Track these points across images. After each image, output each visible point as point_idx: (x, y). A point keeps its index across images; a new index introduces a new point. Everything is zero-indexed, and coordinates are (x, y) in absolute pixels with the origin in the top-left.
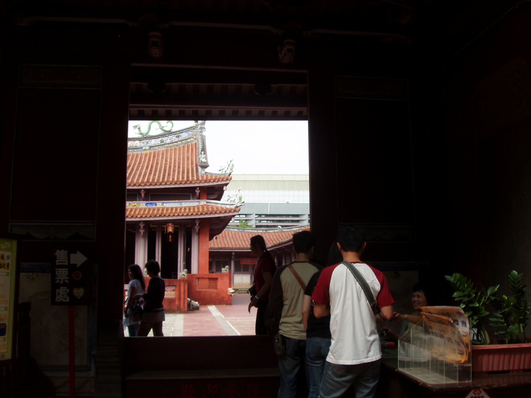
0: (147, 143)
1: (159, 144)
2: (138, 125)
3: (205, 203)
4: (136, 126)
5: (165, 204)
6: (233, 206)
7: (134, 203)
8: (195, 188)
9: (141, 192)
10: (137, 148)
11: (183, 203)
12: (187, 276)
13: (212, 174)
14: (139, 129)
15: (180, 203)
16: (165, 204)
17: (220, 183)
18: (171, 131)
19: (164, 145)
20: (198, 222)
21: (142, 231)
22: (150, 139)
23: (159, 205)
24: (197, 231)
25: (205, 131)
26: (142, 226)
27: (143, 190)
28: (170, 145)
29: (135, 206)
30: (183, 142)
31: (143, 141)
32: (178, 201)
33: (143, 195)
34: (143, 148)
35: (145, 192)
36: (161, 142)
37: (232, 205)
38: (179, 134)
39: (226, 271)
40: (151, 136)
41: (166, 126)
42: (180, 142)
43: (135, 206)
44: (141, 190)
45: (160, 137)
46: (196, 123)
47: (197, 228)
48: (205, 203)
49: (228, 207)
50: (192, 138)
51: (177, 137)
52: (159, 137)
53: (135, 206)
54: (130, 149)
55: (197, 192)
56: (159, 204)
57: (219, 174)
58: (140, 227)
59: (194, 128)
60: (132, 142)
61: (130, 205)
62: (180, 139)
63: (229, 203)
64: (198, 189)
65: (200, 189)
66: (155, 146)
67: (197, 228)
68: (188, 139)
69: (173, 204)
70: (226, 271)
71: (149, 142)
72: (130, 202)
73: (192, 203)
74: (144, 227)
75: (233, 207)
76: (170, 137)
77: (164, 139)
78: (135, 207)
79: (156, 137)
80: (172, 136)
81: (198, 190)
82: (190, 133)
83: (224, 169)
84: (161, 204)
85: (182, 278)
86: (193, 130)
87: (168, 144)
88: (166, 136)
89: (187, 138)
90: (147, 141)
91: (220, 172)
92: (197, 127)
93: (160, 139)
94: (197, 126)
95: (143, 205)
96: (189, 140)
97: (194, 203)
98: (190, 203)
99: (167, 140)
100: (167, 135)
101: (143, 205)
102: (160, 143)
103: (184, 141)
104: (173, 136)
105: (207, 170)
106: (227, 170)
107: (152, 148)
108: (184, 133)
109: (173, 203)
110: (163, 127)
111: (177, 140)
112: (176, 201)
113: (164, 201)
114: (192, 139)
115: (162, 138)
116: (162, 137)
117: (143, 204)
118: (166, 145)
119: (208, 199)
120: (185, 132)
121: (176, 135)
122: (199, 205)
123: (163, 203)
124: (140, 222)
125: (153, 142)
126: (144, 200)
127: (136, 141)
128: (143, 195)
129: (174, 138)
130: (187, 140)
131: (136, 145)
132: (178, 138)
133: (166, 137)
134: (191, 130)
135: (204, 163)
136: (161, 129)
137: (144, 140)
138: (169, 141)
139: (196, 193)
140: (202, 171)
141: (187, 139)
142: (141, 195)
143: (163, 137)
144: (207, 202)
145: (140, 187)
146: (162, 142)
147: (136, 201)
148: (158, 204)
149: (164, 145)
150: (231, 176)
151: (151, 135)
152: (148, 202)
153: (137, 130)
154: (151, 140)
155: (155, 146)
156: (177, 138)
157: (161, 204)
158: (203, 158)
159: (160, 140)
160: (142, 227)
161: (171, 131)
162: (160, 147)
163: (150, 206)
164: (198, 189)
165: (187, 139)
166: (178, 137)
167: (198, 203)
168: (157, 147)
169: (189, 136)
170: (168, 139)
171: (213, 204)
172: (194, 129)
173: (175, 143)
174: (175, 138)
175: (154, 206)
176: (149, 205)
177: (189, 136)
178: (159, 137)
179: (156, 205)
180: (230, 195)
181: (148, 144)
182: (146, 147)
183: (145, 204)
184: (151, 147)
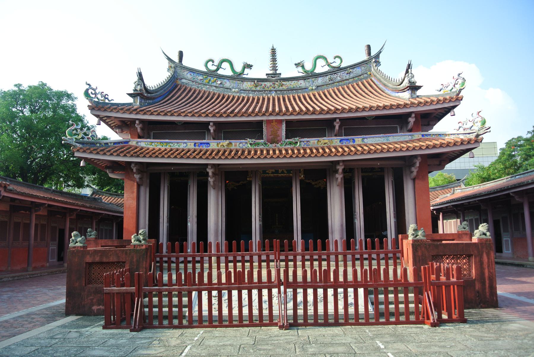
0: (313, 82)
1: (327, 83)
2: (301, 62)
3: (420, 137)
4: (299, 63)
5: (366, 139)
6: (471, 135)
7: (324, 140)
8: (409, 115)
9: (335, 123)
10: (301, 89)
11: (390, 137)
12: (490, 236)
13: (428, 97)
14: (303, 67)
15: (386, 138)
16: (365, 140)
17: (446, 105)
18: (341, 67)
19: (333, 83)
20: (420, 161)
21: (339, 176)
22: (316, 78)
23: (359, 141)
24: (415, 173)
25: (380, 65)
26: (340, 168)
27: (338, 120)
28: (340, 83)
29: (325, 143)
30: (355, 79)
31: (308, 80)
32: (383, 135)
33: (337, 127)
34: (310, 88)
35: (340, 123)
36: (330, 81)
37: (469, 134)
38: (351, 70)
39: (465, 228)
40: (317, 74)
41: (334, 62)
42: (352, 80)
43: (327, 143)
44: (335, 119)
45: (327, 75)
46: (369, 57)
47: (415, 170)
48: (420, 137)
49: (462, 137)
50: (366, 73)
51: (347, 74)
52: (327, 74)
53: (327, 143)
54: (294, 90)
55: (412, 120)
56: (358, 140)
57: (439, 95)
58: (336, 171)
59: (367, 62)
60: (296, 82)
61: (319, 142)
62: (352, 75)
63: (461, 131)
64: (413, 115)
65: (416, 117)
66: (323, 85)
67: (415, 170)
68: (360, 76)
69: (377, 139)
70: (465, 228)
71: (314, 82)
72: (319, 139)
73: (402, 137)
74: (344, 170)
75: (472, 136)
76: (339, 74)
77: (332, 76)
78: (326, 145)
79: (323, 75)
80: (341, 73)
81: (413, 118)
82: (363, 68)
83: (438, 90)
84: (360, 139)
85: (483, 239)
86: (366, 65)
87: (338, 82)
88: (335, 74)
89: (360, 74)
90: (313, 79)
91: (442, 92)
92: (371, 62)
93: (329, 76)
94: (370, 60)
95: (336, 142)
96: (362, 77)
97: (405, 137)
98: (400, 137)
99: (338, 77)
100: (336, 72)
101: (336, 142)
102: (328, 81)
103: (357, 78)
104: (343, 72)
105: (419, 93)
106: (454, 88)
107: (319, 88)
108: (355, 69)
109: (377, 138)
110: (331, 63)
111: (348, 77)
112: (381, 135)
113: (364, 136)
114: (365, 75)
115: (331, 76)
116: (330, 75)
117: (336, 140)
118: (335, 84)
119: (422, 131)
120: (356, 68)
121: (347, 72)
122: (412, 139)
123: (363, 139)
124: (338, 162)
125: (320, 81)
126: (336, 136)
127: (300, 81)
128: (337, 127)
129: (343, 75)
130: (360, 77)
131: (300, 85)
132: (349, 76)
133: (335, 75)
134: (364, 65)
135: (413, 84)
136: (328, 65)
137: (309, 79)
138: (339, 78)
139: (408, 123)
140: (413, 94)
141: (359, 76)
142: (334, 127)
143: (331, 74)
144: (423, 135)
145: (335, 116)
146: (331, 79)
147: (325, 136)
148: (356, 140)
149: (333, 83)
150: (460, 95)
151: (317, 73)
152: (343, 137)
153: (300, 69)
154: (317, 79)
155: (323, 85)
156: (348, 74)
157: (360, 139)
158: (410, 77)
159: (329, 78)
160: (340, 171)
161: (341, 67)
162: (328, 86)
163: (345, 143)
164: (413, 115)
165: (359, 76)
166: (349, 73)
167: (410, 136)
168: (325, 86)
169: (363, 72)
170: (337, 77)
171: (433, 137)
172: (366, 64)
173: (346, 81)
174: (346, 75)
175: (352, 143)
176: (345, 141)
177: (362, 71)
178: (327, 74)
179: (354, 141)
180: (462, 122)
181: (314, 84)
182: (312, 87)
183: (339, 140)
184: (318, 87)
